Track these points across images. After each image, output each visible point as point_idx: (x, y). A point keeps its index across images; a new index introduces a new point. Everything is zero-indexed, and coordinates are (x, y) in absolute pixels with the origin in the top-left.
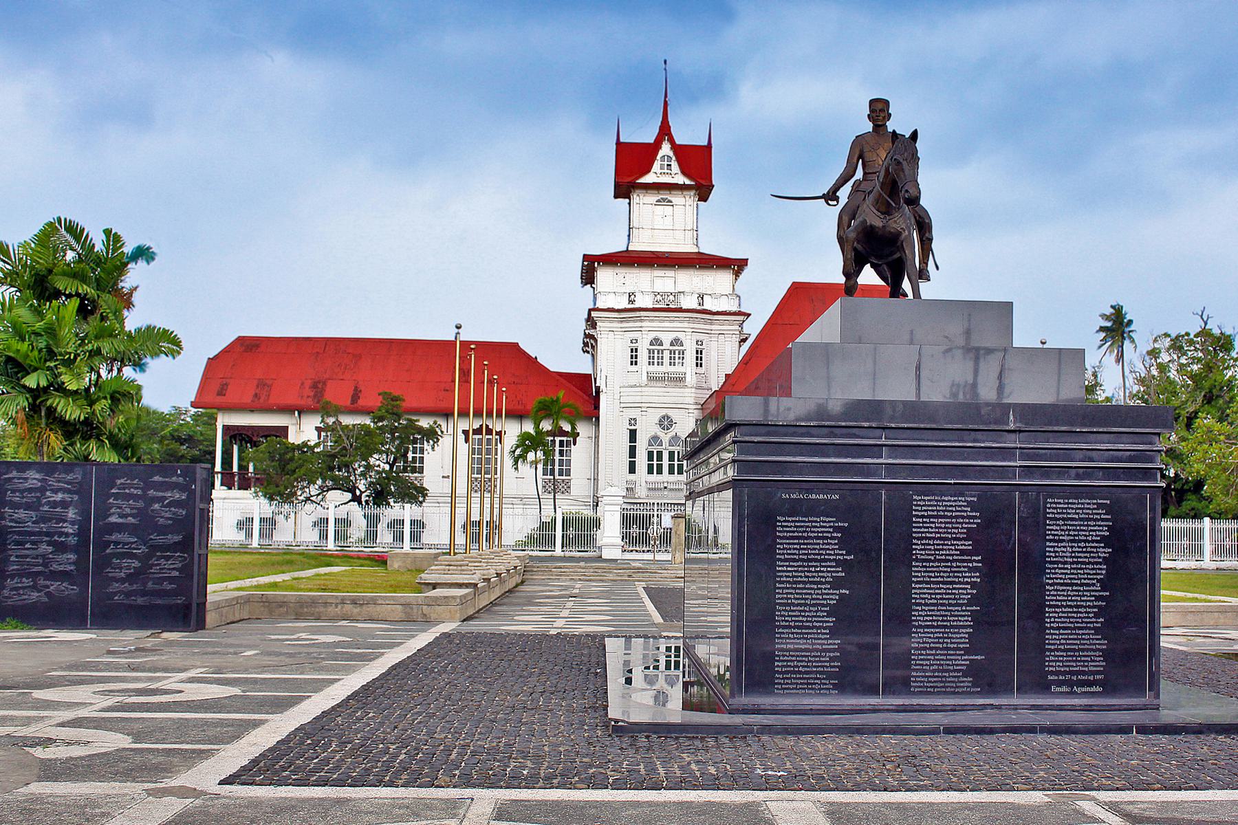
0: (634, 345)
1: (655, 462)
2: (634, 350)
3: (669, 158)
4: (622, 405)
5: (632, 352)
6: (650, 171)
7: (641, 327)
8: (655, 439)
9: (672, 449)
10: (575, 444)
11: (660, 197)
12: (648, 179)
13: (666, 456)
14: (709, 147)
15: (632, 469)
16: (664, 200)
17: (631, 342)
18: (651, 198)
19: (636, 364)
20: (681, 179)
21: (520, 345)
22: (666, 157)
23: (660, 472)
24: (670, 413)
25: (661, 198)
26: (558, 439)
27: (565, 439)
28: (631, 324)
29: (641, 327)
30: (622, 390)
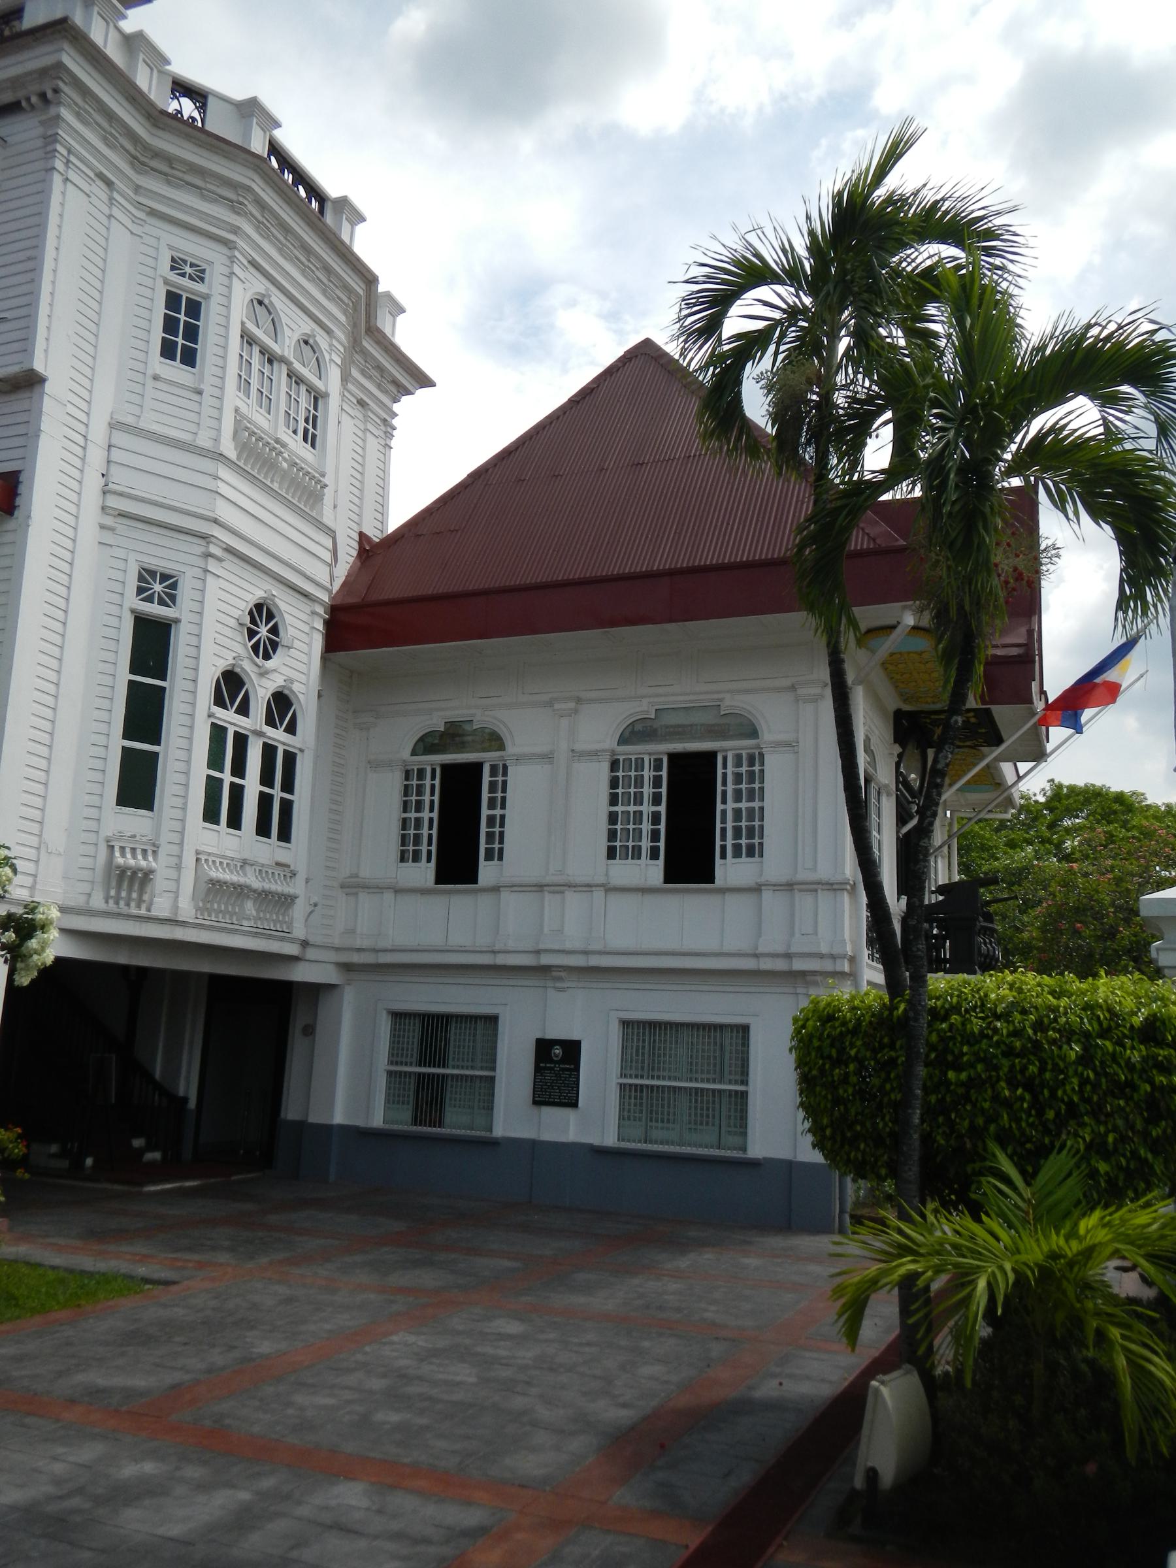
4: (113, 502)
5: (173, 300)
7: (236, 230)
17: (176, 265)
19: (189, 358)
30: (120, 438)
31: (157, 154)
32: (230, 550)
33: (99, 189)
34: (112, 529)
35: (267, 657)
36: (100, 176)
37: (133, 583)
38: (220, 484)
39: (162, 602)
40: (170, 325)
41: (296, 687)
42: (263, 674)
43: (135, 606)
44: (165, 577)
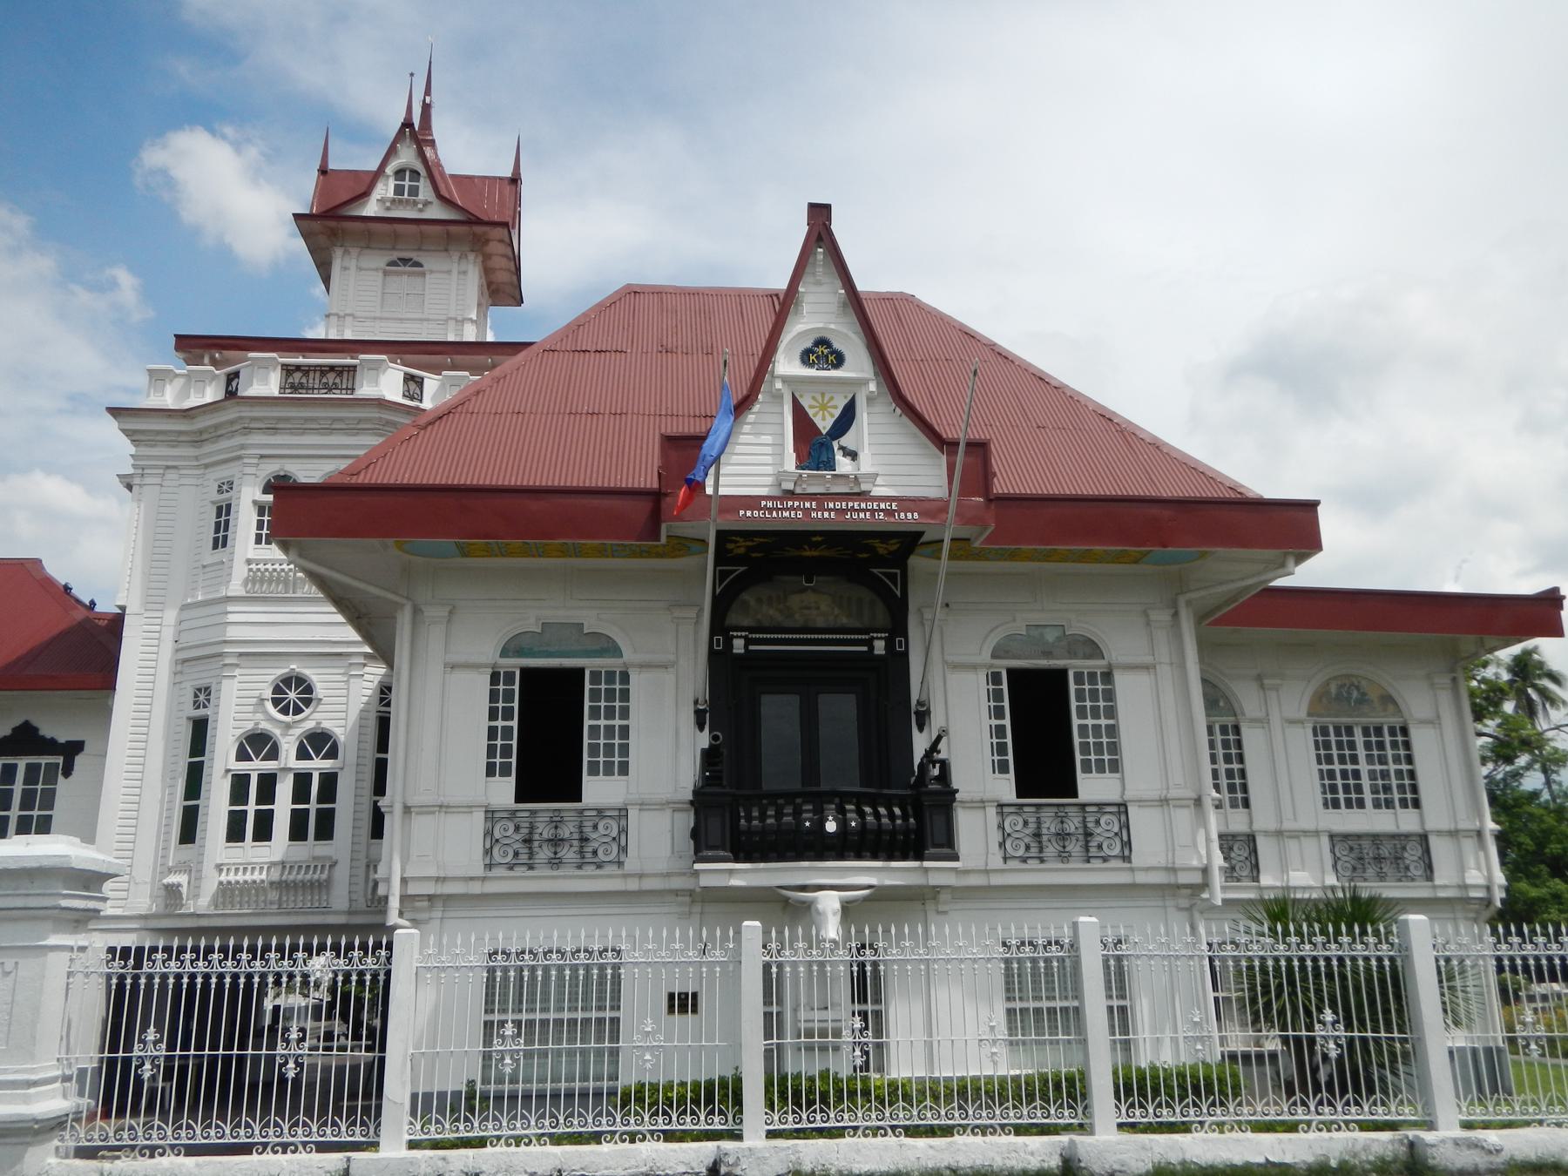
0: (225, 495)
1: (251, 807)
2: (224, 513)
3: (415, 174)
5: (219, 509)
6: (366, 194)
7: (243, 447)
8: (258, 743)
9: (304, 765)
10: (68, 772)
11: (395, 255)
12: (371, 208)
13: (284, 790)
14: (515, 180)
15: (189, 832)
16: (405, 261)
17: (220, 491)
18: (378, 260)
19: (224, 545)
20: (436, 212)
21: (43, 562)
22: (408, 173)
23: (264, 831)
24: (312, 674)
25: (400, 259)
26: (22, 763)
27: (44, 760)
28: (224, 444)
29: (243, 447)
30: (187, 614)
31: (201, 432)
32: (241, 655)
33: (171, 475)
34: (181, 672)
35: (298, 711)
36: (168, 467)
37: (190, 698)
38: (230, 616)
39: (205, 706)
40: (218, 525)
41: (326, 725)
42: (288, 726)
43: (191, 715)
44: (206, 689)
